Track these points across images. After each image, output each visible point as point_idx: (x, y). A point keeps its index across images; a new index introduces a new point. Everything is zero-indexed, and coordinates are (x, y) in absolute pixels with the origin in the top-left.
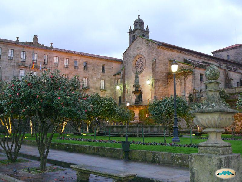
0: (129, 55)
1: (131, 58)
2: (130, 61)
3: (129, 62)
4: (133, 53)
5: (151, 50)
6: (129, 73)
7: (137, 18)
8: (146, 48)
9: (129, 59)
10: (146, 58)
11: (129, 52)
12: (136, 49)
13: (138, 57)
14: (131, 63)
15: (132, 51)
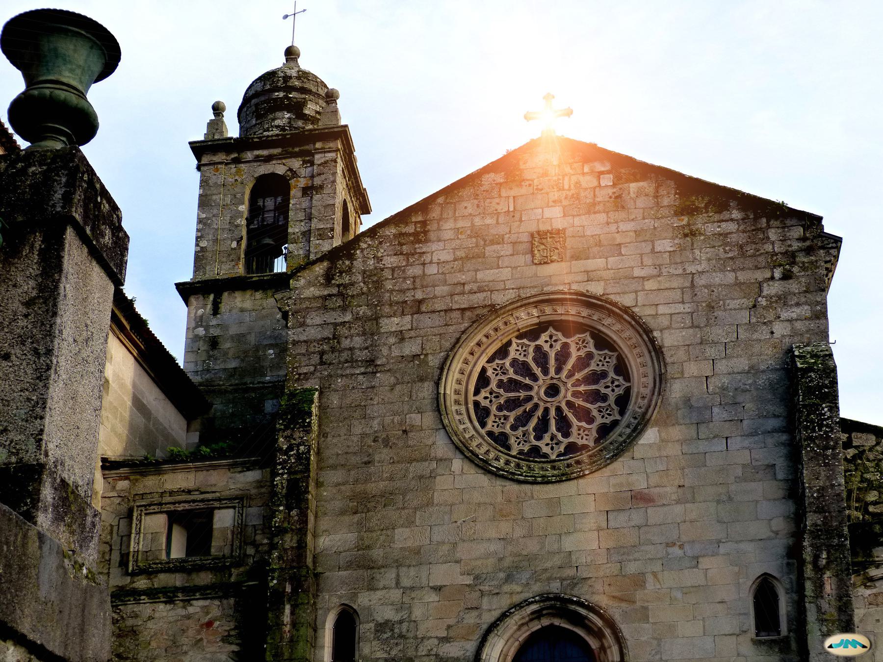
0: (389, 285)
1: (426, 321)
2: (411, 348)
3: (390, 351)
4: (462, 278)
5: (742, 276)
6: (384, 454)
7: (277, 61)
8: (665, 245)
9: (391, 324)
10: (668, 340)
11: (390, 261)
12: (507, 249)
13: (526, 318)
14: (434, 361)
15: (445, 256)
